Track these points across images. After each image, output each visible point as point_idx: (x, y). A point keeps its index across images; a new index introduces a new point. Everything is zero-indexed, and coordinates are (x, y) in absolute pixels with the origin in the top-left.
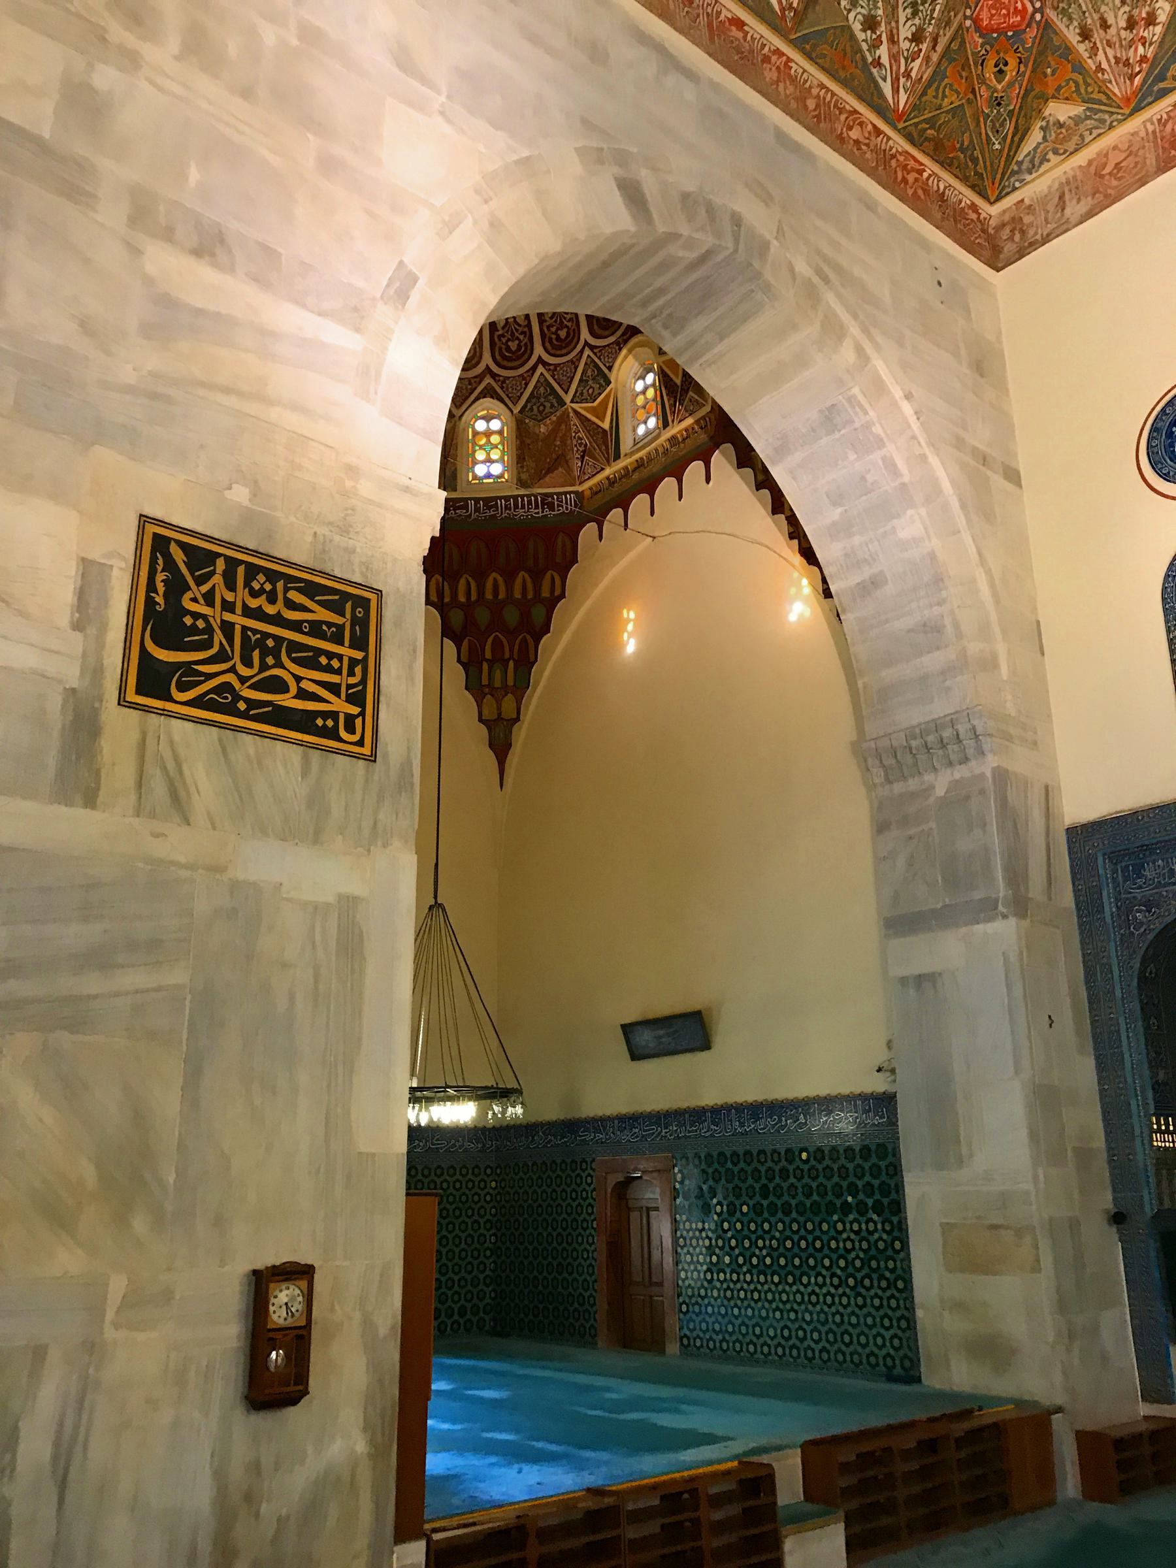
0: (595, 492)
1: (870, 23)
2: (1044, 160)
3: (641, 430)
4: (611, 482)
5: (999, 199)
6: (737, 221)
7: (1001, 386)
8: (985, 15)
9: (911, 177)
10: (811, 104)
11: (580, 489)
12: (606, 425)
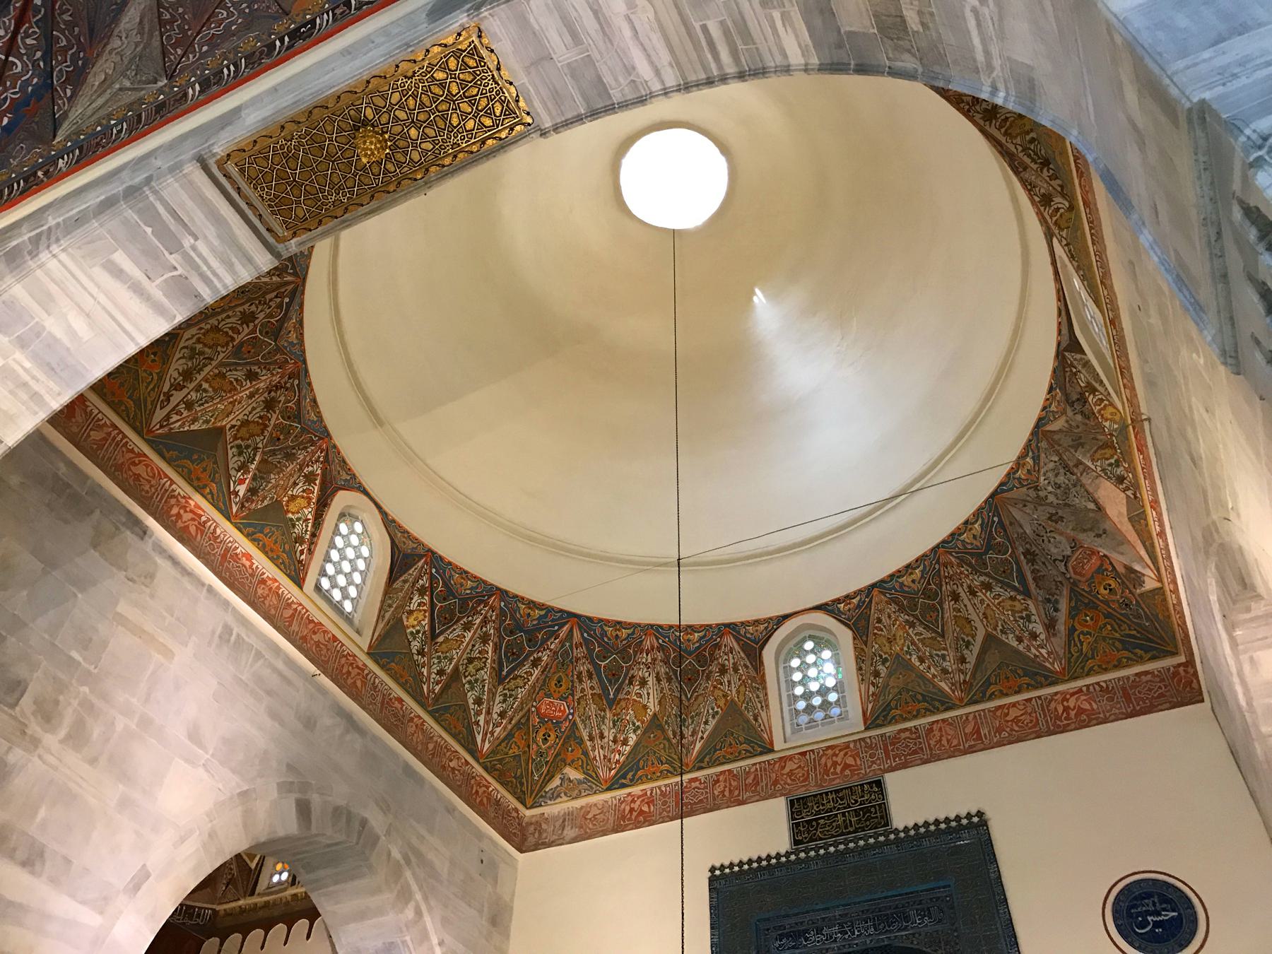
0: (228, 914)
1: (478, 701)
2: (559, 796)
3: (276, 879)
4: (242, 910)
5: (532, 807)
6: (364, 823)
7: (506, 935)
8: (543, 707)
9: (481, 791)
10: (431, 746)
11: (218, 908)
12: (253, 866)
